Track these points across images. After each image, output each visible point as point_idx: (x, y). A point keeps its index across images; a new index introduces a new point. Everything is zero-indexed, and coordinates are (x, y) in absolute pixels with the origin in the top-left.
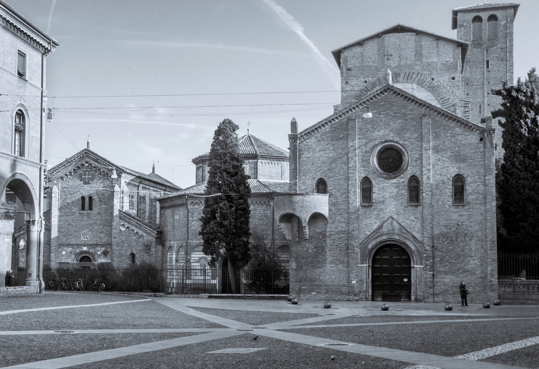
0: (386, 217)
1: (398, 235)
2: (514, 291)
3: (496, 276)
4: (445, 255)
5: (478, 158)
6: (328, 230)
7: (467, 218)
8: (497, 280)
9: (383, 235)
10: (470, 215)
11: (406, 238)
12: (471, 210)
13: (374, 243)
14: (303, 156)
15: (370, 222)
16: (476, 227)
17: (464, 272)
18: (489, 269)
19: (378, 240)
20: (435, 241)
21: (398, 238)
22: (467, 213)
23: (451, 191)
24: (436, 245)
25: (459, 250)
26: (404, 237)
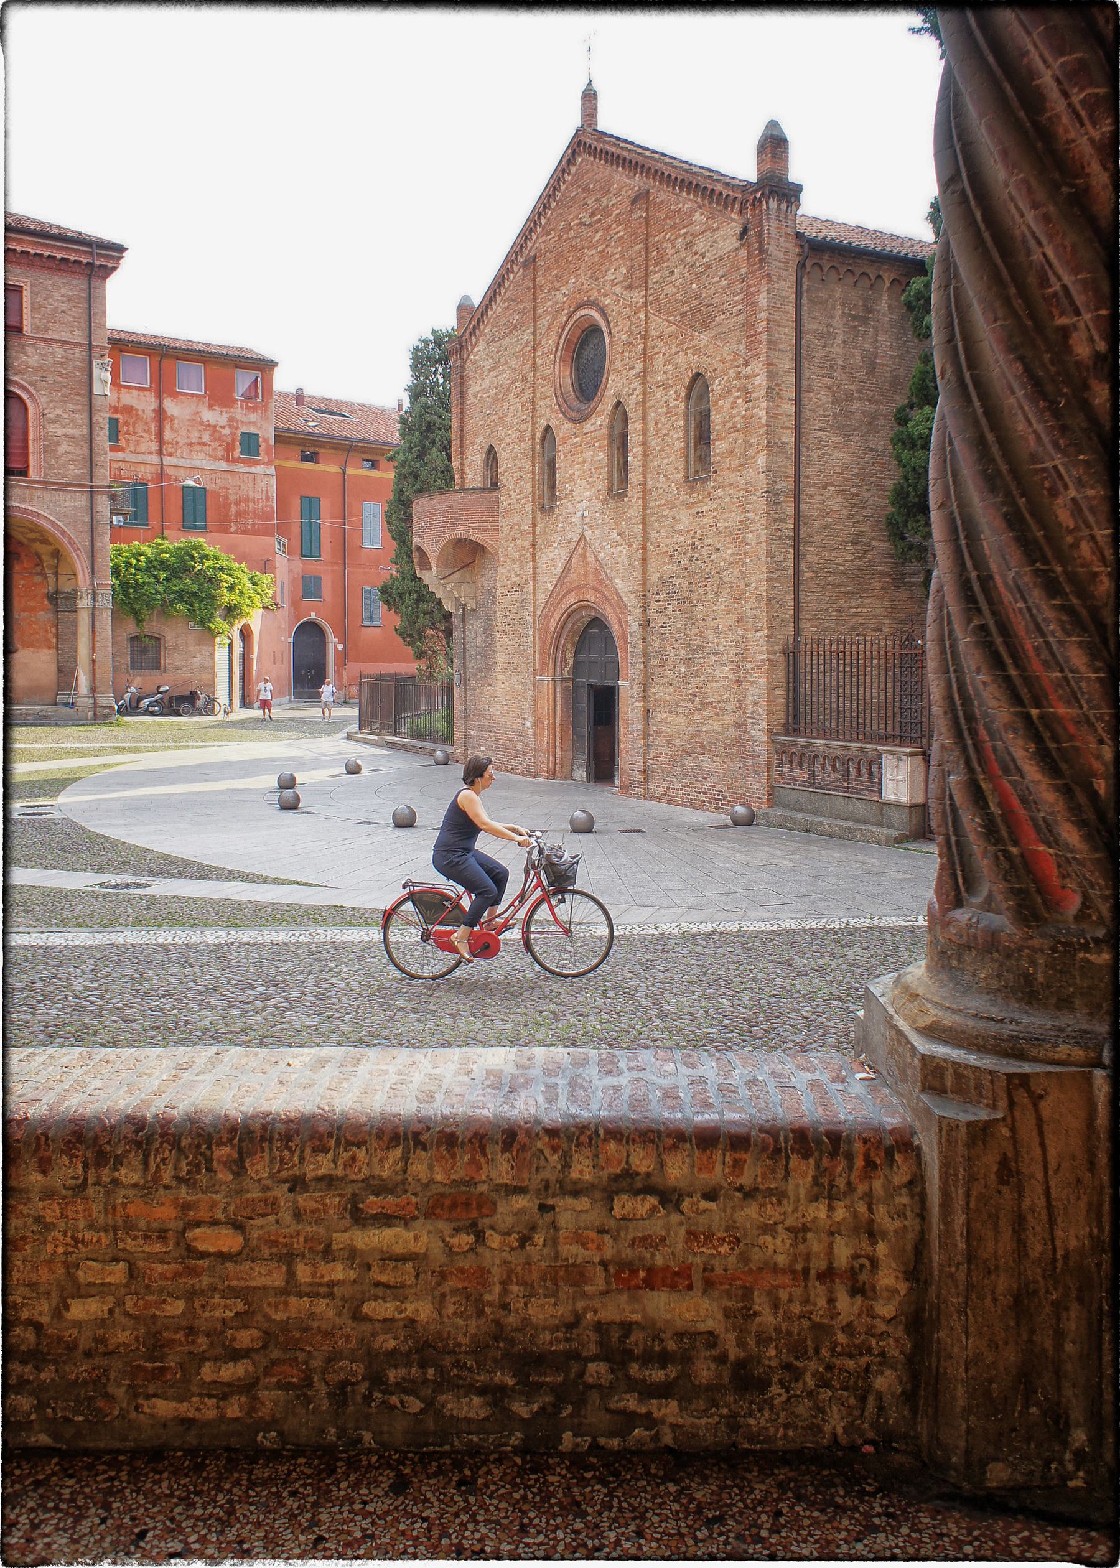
0: (576, 538)
1: (594, 589)
2: (812, 782)
3: (764, 725)
4: (668, 648)
5: (736, 303)
6: (499, 583)
7: (711, 522)
8: (765, 739)
9: (571, 590)
10: (716, 509)
11: (606, 599)
12: (720, 492)
13: (557, 616)
14: (471, 392)
15: (551, 555)
16: (729, 551)
17: (703, 704)
18: (749, 697)
19: (565, 607)
20: (652, 605)
21: (593, 598)
22: (713, 505)
23: (681, 434)
24: (653, 616)
25: (694, 631)
26: (602, 593)
